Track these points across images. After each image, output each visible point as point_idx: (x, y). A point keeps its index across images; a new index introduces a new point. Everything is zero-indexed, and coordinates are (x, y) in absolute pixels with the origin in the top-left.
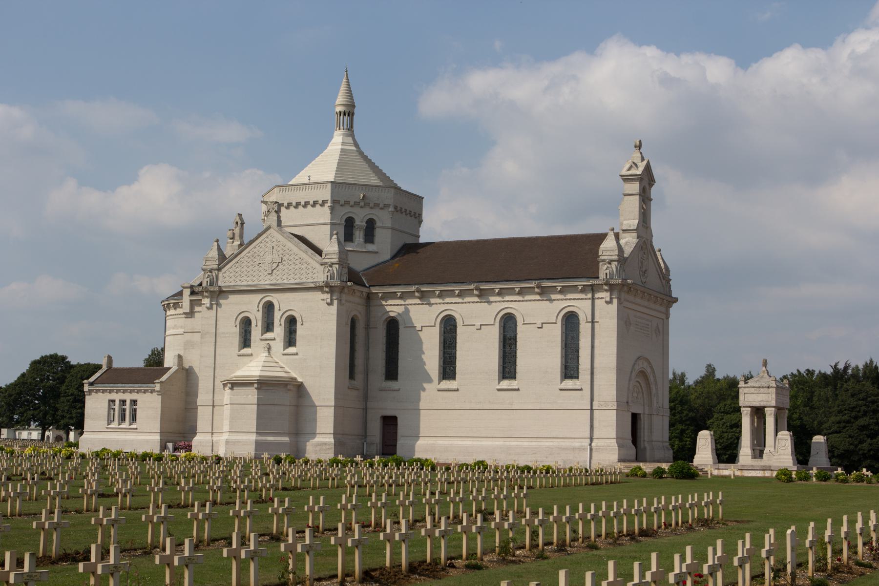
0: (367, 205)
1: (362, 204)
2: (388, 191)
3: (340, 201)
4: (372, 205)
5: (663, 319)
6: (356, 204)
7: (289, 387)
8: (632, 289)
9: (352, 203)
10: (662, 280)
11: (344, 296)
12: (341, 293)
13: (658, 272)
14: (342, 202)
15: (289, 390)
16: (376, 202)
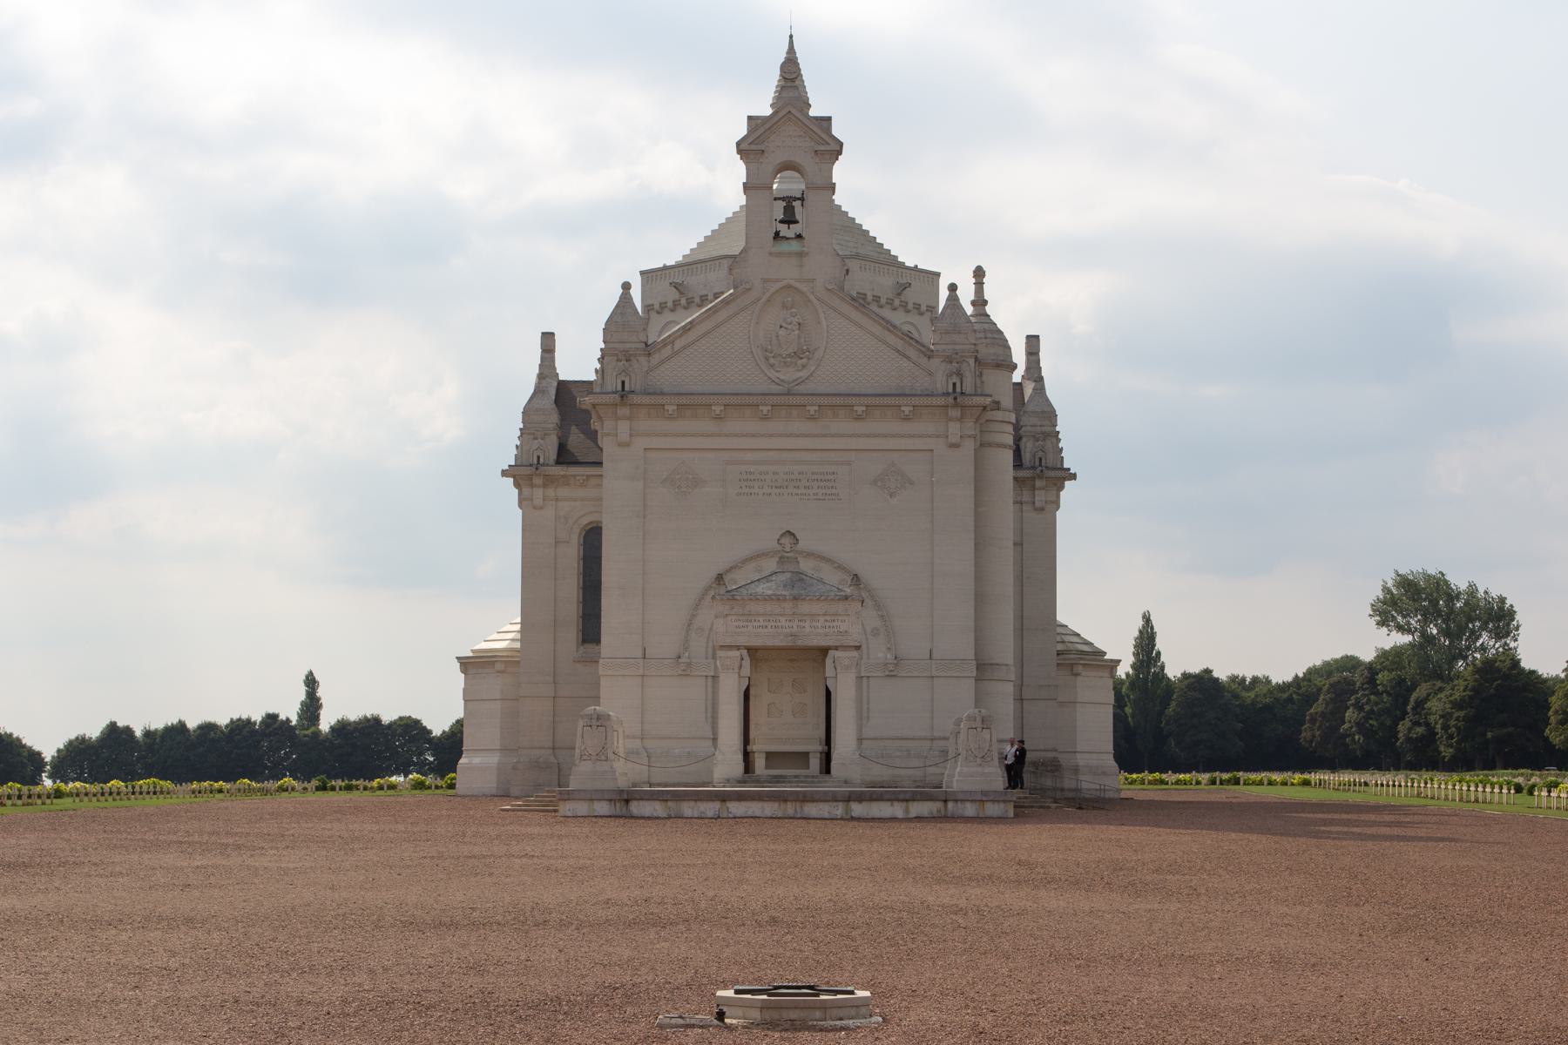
0: (690, 302)
1: (683, 302)
2: (720, 266)
3: (653, 305)
4: (697, 300)
5: (932, 450)
6: (676, 304)
7: (499, 667)
8: (671, 408)
9: (670, 304)
10: (923, 360)
11: (538, 493)
12: (532, 486)
13: (885, 343)
14: (657, 307)
15: (498, 672)
16: (705, 292)
